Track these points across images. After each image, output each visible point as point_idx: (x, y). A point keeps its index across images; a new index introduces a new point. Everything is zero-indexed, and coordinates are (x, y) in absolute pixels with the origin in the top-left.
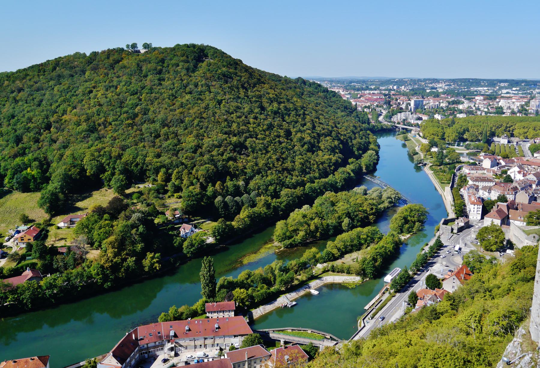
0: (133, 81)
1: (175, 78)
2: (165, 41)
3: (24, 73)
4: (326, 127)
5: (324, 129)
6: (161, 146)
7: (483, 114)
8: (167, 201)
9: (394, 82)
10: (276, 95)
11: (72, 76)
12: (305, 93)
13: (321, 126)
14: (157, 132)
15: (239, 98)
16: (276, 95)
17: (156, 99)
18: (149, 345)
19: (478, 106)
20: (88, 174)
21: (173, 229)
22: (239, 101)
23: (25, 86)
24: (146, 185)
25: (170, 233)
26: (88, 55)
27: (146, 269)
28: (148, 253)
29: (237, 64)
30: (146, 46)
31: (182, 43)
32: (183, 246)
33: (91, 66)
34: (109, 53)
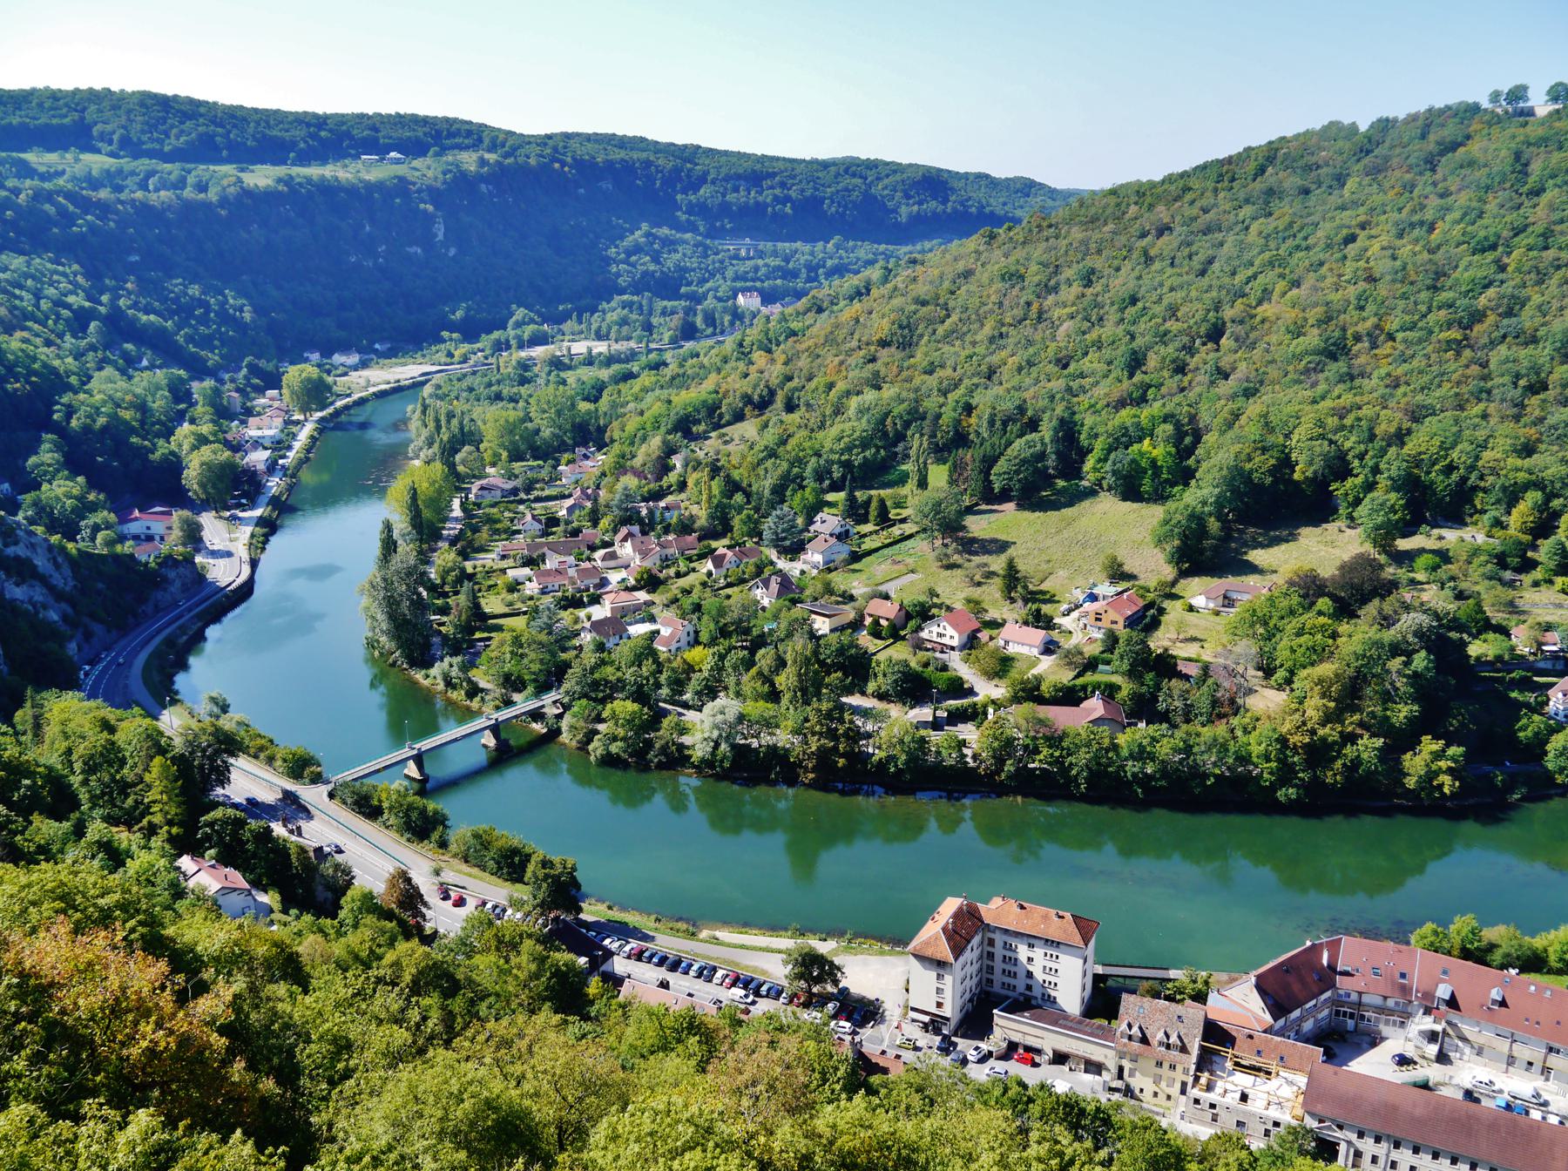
0: (1491, 207)
3: (1181, 183)
6: (1542, 420)
8: (1527, 595)
14: (1538, 374)
17: (1558, 268)
18: (1366, 999)
20: (1297, 476)
21: (1526, 684)
23: (1178, 218)
24: (1467, 533)
25: (1514, 695)
27: (1411, 782)
28: (1426, 739)
32: (1549, 747)
33: (1366, 161)
34: (1428, 121)
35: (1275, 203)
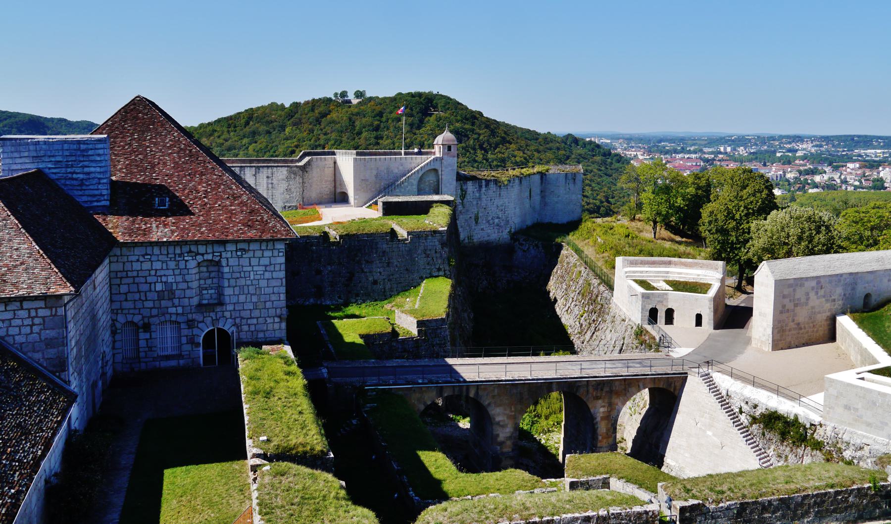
0: (345, 139)
1: (396, 136)
2: (382, 87)
3: (210, 128)
4: (591, 201)
5: (588, 204)
7: (850, 189)
9: (729, 140)
10: (525, 159)
11: (269, 132)
12: (573, 156)
13: (585, 199)
15: (476, 161)
16: (525, 159)
19: (846, 178)
22: (475, 165)
26: (287, 105)
29: (475, 118)
30: (359, 94)
31: (404, 92)
35: (257, 137)
